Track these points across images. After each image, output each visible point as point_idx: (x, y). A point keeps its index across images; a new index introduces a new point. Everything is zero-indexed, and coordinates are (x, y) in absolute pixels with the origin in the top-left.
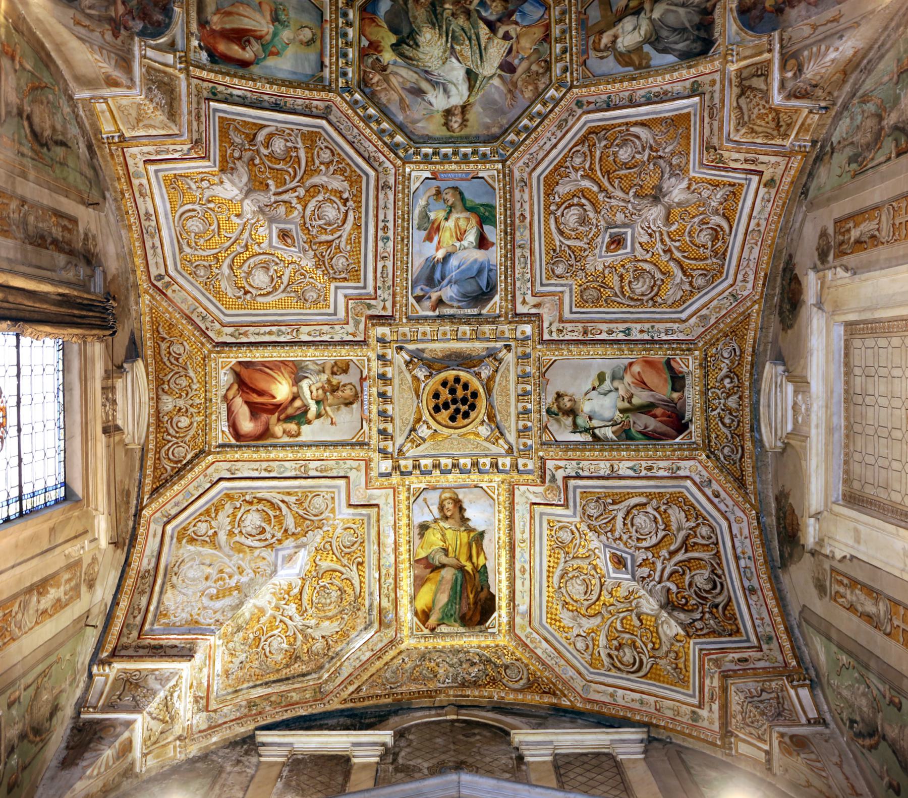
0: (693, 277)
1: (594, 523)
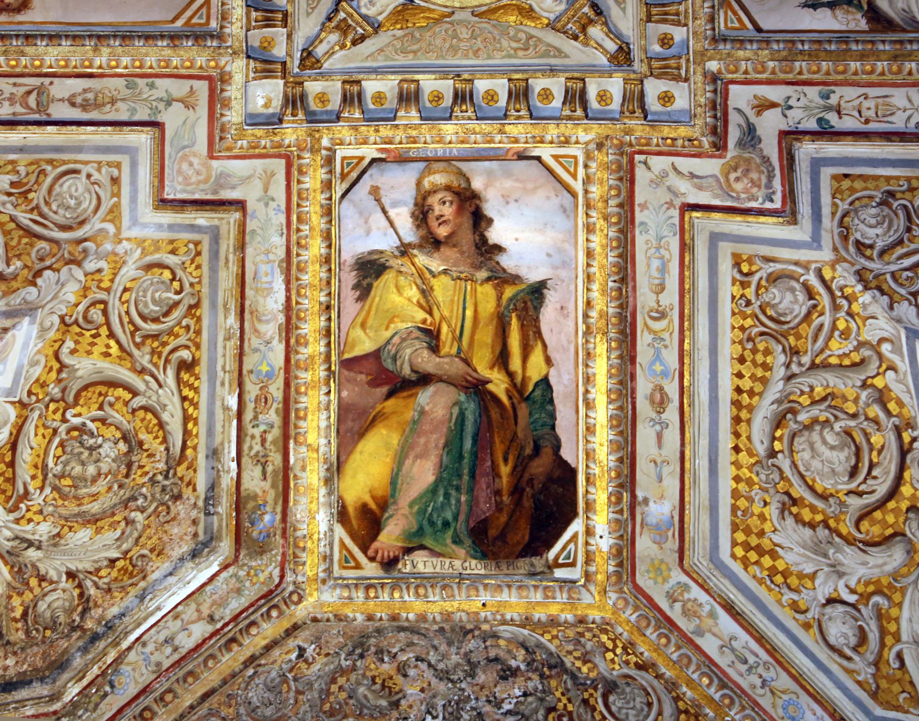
1: (876, 266)
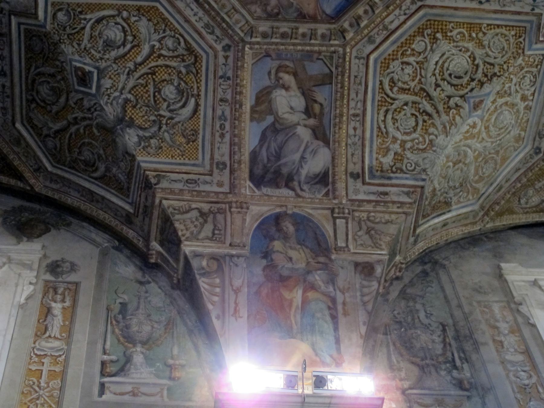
0: (54, 138)
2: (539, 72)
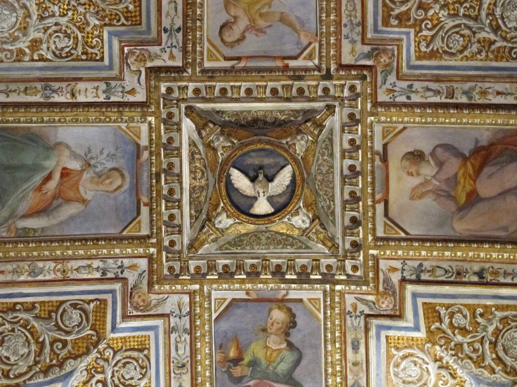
2: (78, 59)
